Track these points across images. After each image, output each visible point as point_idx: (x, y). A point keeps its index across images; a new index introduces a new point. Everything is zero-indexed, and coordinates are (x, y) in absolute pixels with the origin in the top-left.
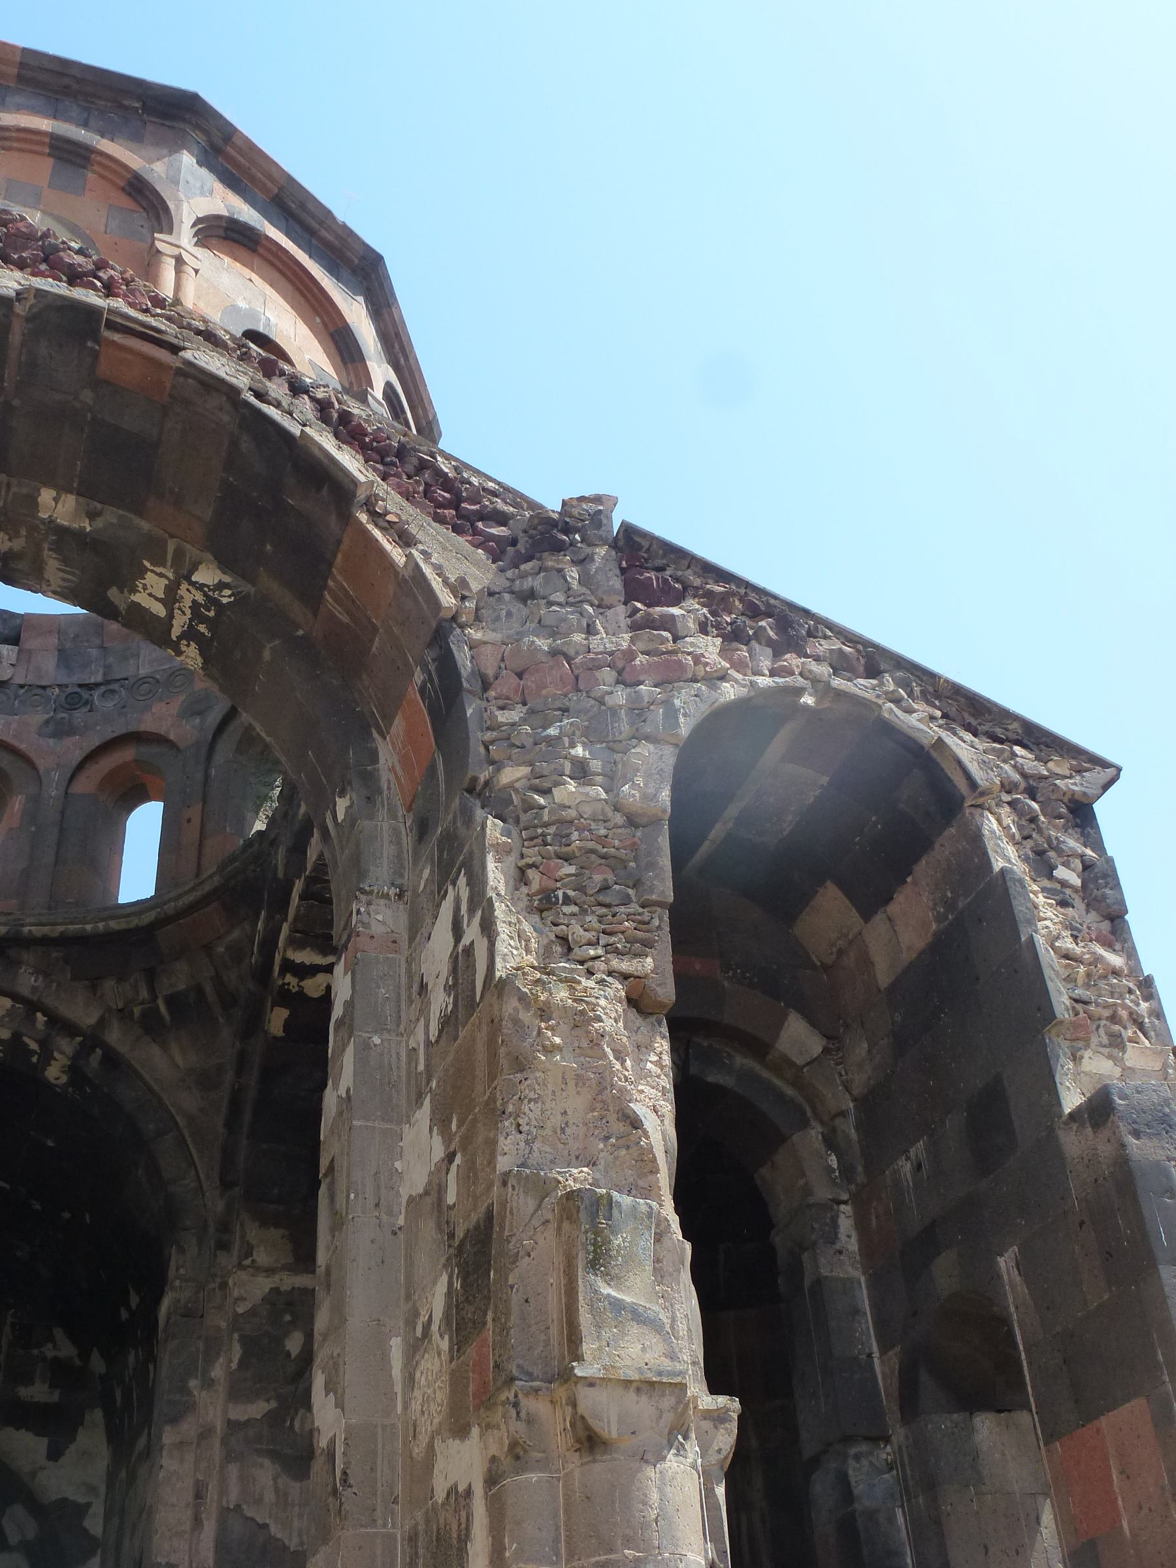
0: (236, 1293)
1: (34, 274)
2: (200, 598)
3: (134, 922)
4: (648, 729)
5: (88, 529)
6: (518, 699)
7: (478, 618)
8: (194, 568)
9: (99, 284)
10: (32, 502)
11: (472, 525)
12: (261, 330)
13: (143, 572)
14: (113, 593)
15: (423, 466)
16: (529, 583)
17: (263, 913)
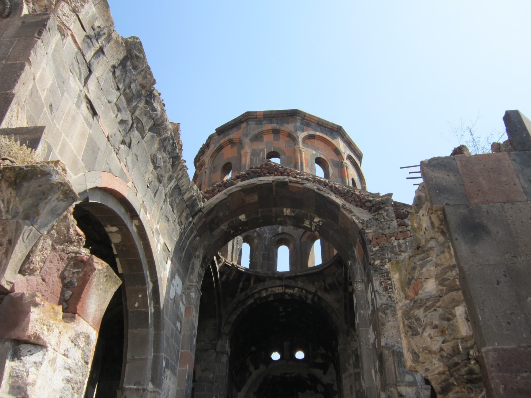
0: (352, 346)
1: (275, 175)
2: (316, 224)
3: (318, 270)
4: (402, 249)
5: (293, 215)
6: (377, 244)
7: (367, 227)
8: (314, 219)
9: (286, 174)
10: (283, 212)
11: (364, 204)
12: (319, 156)
13: (305, 221)
14: (300, 224)
15: (353, 193)
16: (377, 217)
17: (343, 267)
